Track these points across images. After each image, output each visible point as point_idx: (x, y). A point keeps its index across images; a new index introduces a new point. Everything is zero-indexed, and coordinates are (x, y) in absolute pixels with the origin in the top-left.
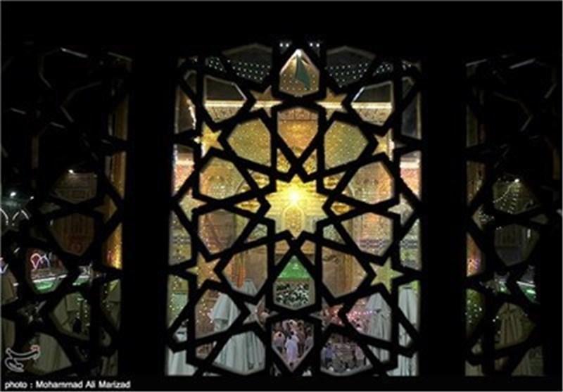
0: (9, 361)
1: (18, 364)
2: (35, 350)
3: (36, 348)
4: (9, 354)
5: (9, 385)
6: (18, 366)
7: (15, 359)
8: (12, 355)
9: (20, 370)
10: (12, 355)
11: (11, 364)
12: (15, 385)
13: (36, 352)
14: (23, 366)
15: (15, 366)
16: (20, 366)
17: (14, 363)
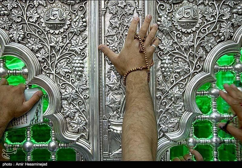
0: (3, 154)
1: (8, 156)
2: (14, 150)
3: (16, 149)
4: (4, 151)
5: (4, 165)
6: (7, 157)
7: (5, 153)
8: (6, 152)
9: (8, 158)
10: (5, 151)
11: (4, 156)
12: (7, 165)
13: (15, 151)
14: (9, 157)
15: (7, 157)
16: (8, 157)
17: (6, 155)
